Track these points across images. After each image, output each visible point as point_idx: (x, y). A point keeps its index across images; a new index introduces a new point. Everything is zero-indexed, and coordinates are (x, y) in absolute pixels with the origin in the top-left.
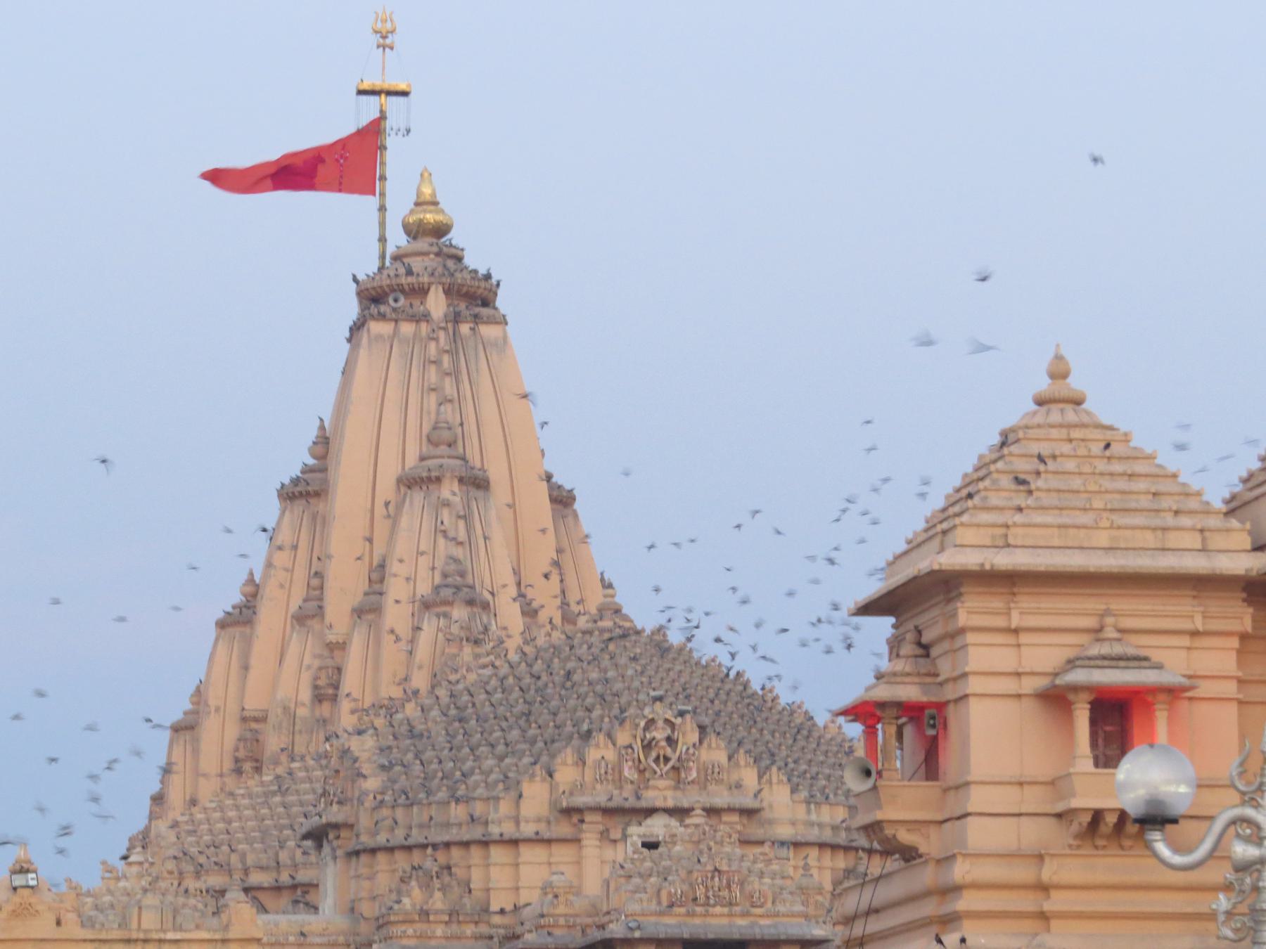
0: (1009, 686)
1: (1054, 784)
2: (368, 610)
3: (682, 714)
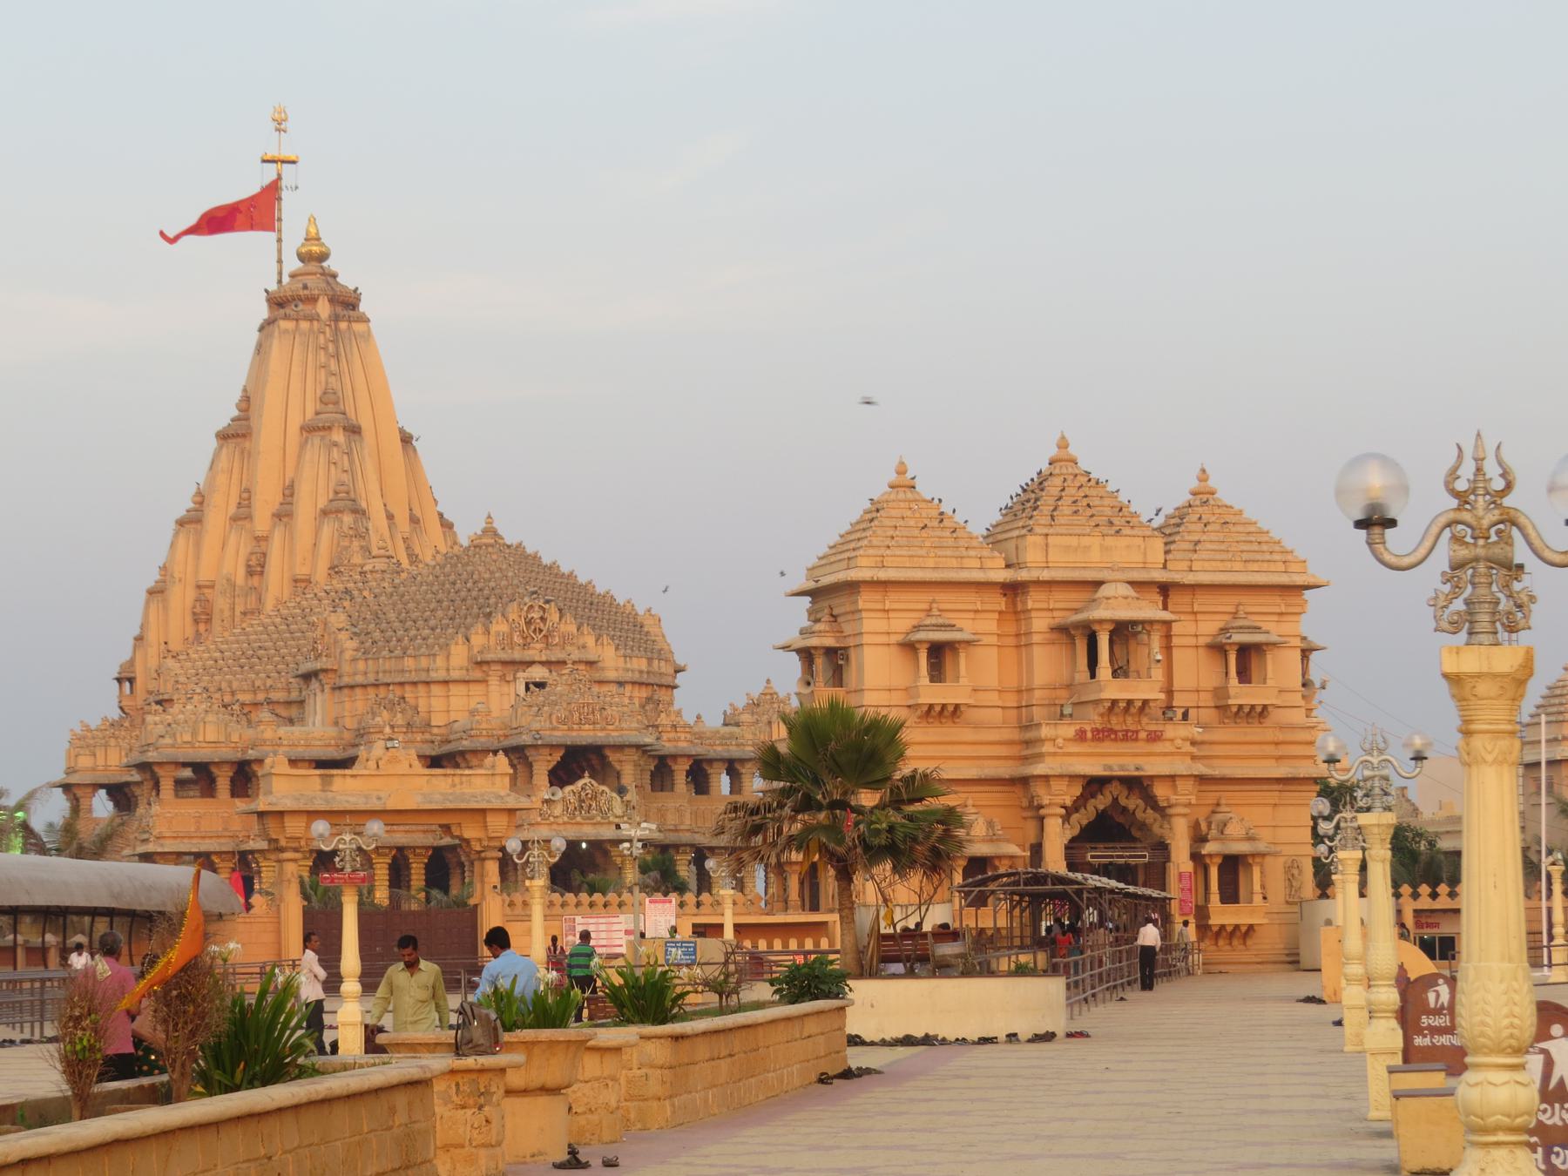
0: (884, 639)
2: (284, 515)
3: (547, 602)
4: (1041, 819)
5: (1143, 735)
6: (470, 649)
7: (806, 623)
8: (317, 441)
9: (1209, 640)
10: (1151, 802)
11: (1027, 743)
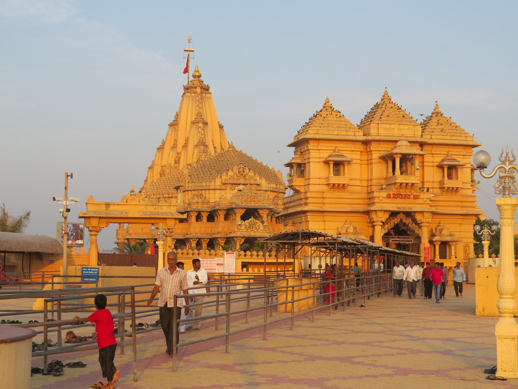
0: (318, 160)
1: (327, 178)
2: (185, 146)
4: (373, 227)
5: (412, 196)
6: (222, 180)
7: (293, 156)
8: (195, 126)
9: (437, 164)
10: (415, 221)
11: (370, 199)
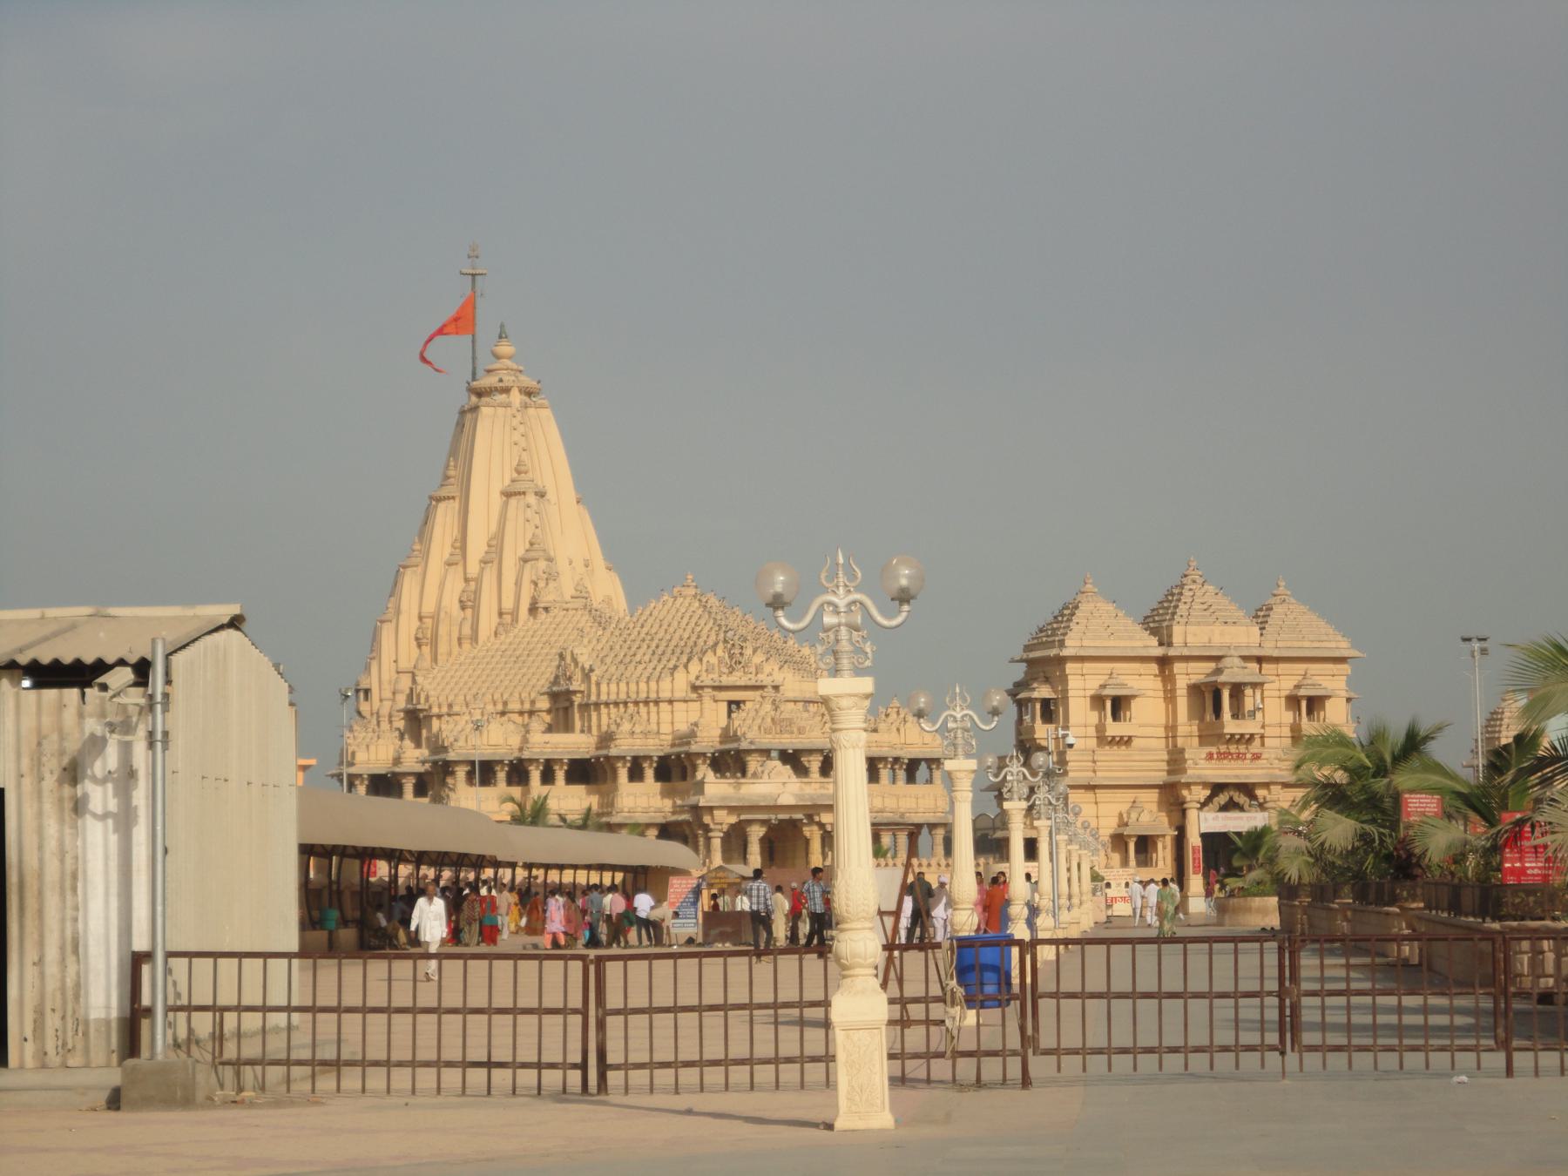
0: (1081, 693)
